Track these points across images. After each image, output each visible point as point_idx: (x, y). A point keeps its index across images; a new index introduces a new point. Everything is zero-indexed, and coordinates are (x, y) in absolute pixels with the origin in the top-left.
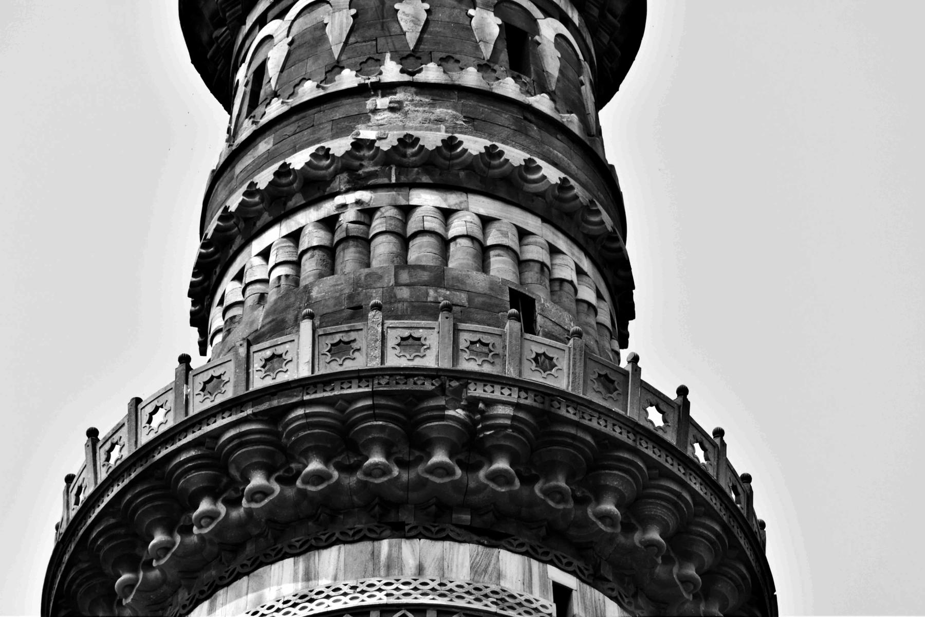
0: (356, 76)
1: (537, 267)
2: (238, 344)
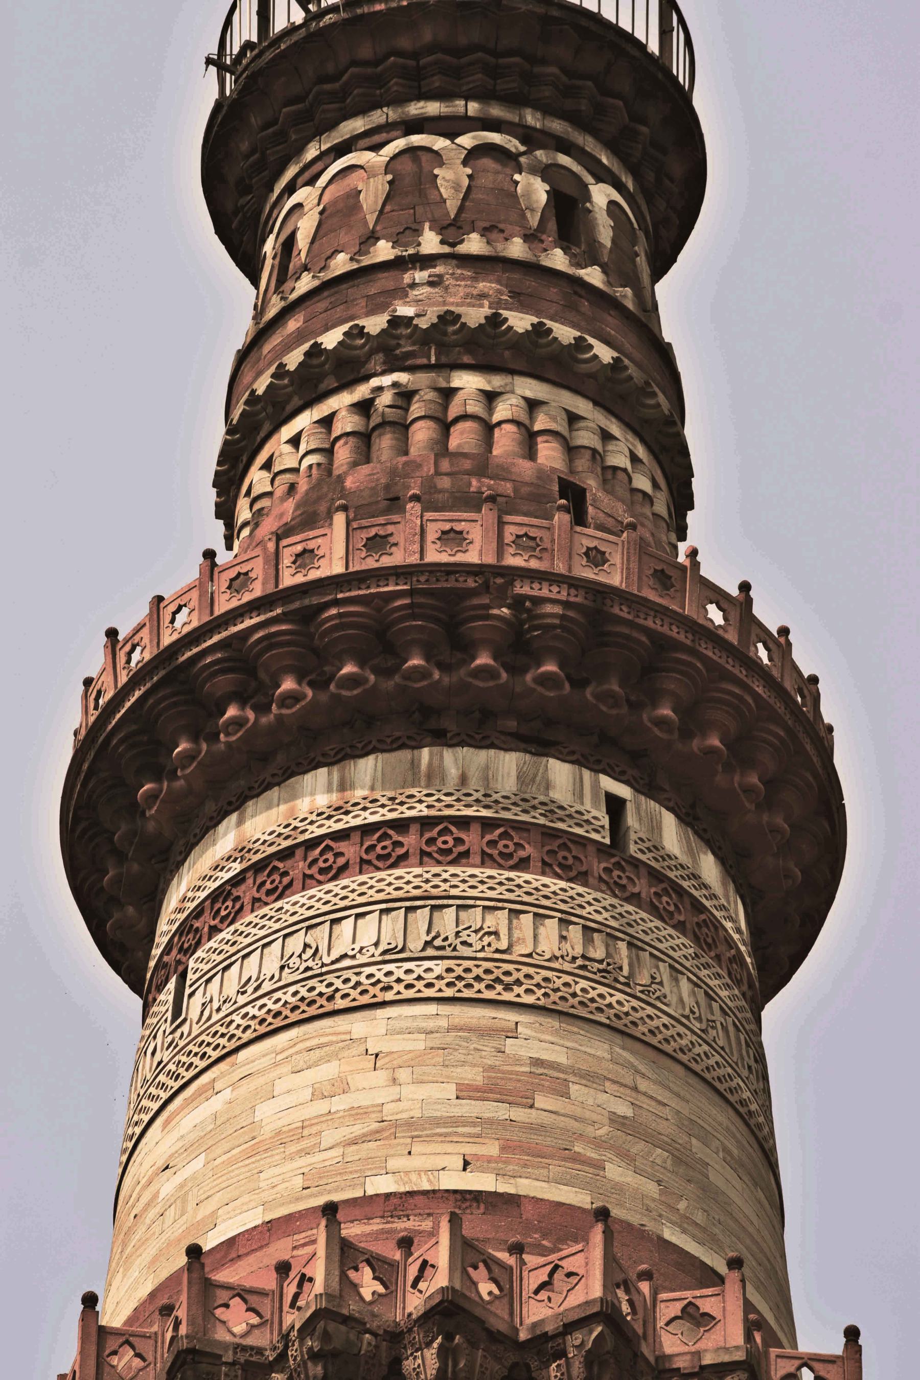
0: (393, 247)
1: (588, 454)
2: (266, 538)
